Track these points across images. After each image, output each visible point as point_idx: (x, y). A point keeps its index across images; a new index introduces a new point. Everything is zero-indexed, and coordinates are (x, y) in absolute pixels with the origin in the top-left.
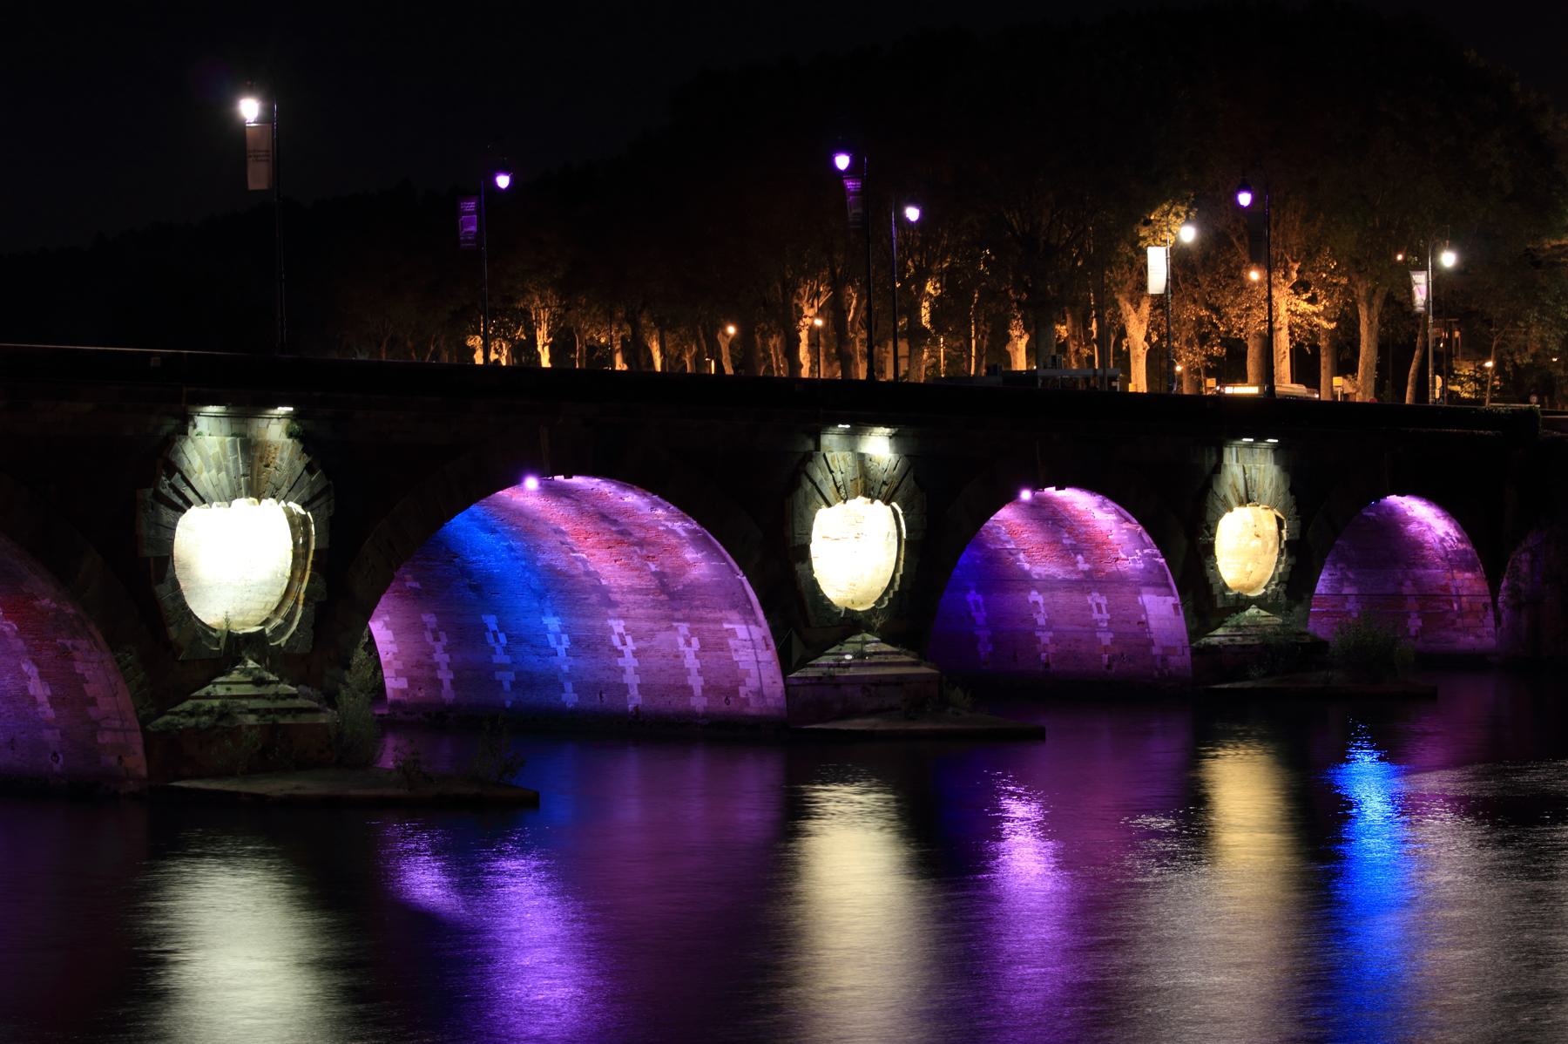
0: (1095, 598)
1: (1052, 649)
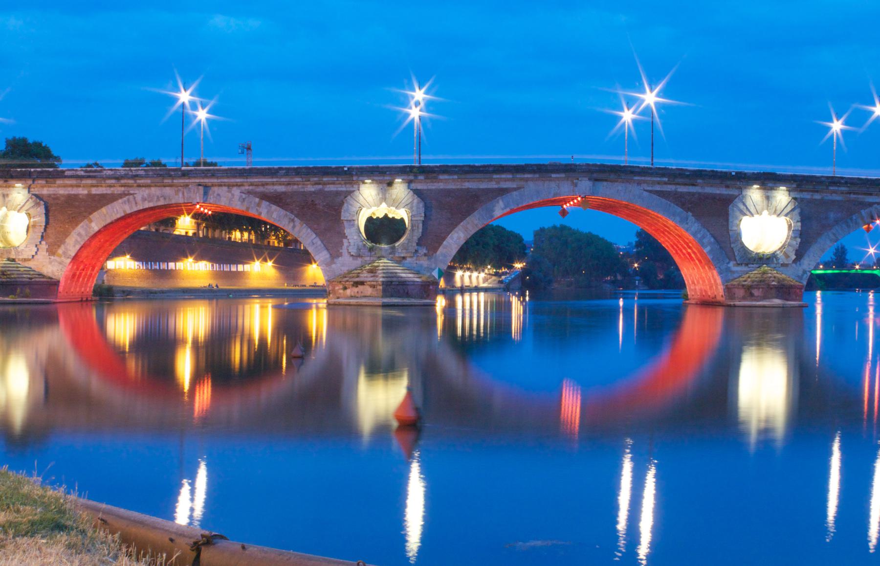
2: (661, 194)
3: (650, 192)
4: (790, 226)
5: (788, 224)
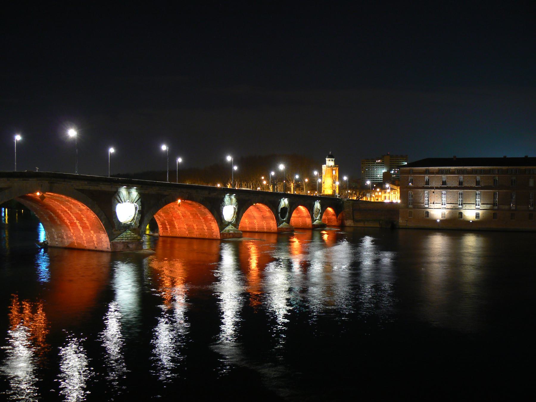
0: (300, 219)
1: (294, 224)
2: (82, 191)
3: (77, 190)
4: (136, 208)
5: (135, 207)
